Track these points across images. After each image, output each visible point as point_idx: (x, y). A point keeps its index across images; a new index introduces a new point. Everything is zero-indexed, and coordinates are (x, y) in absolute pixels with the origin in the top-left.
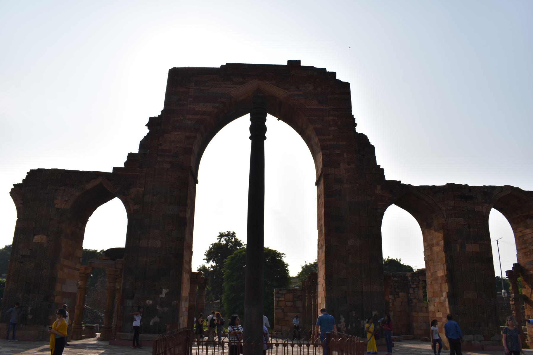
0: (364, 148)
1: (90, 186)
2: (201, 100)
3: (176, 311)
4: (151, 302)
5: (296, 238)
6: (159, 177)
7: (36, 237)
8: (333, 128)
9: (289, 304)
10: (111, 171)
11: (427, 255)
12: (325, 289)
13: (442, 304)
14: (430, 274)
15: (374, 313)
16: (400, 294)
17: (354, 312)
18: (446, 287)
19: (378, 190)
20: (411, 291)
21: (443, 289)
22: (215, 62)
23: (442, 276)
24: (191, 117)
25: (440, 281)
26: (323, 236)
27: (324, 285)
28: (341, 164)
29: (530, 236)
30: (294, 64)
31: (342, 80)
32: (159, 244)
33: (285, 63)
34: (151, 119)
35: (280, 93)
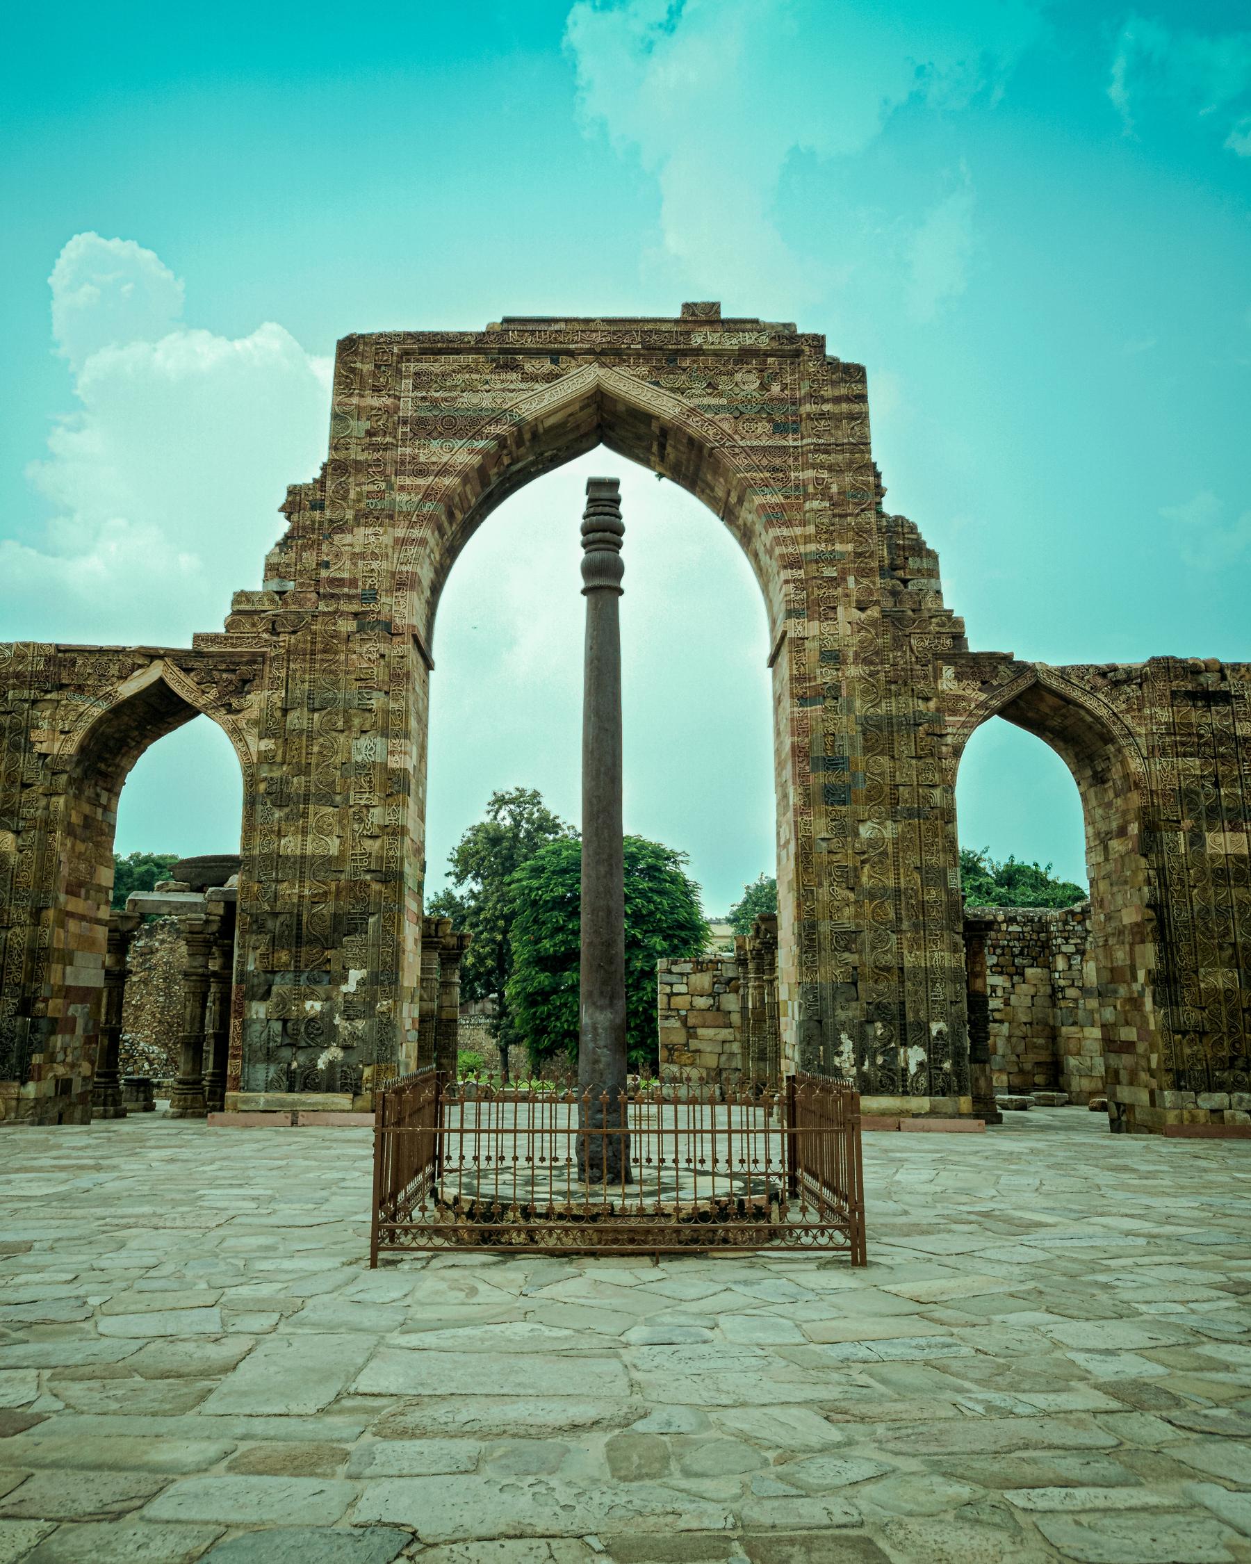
1: (127, 689)
3: (387, 1029)
4: (318, 1006)
5: (720, 816)
14: (1102, 917)
15: (935, 1027)
17: (879, 1025)
19: (948, 680)
23: (1137, 924)
25: (1128, 938)
26: (790, 814)
27: (795, 949)
28: (840, 609)
30: (704, 315)
31: (845, 359)
32: (334, 846)
33: (677, 314)
34: (293, 491)
35: (662, 403)
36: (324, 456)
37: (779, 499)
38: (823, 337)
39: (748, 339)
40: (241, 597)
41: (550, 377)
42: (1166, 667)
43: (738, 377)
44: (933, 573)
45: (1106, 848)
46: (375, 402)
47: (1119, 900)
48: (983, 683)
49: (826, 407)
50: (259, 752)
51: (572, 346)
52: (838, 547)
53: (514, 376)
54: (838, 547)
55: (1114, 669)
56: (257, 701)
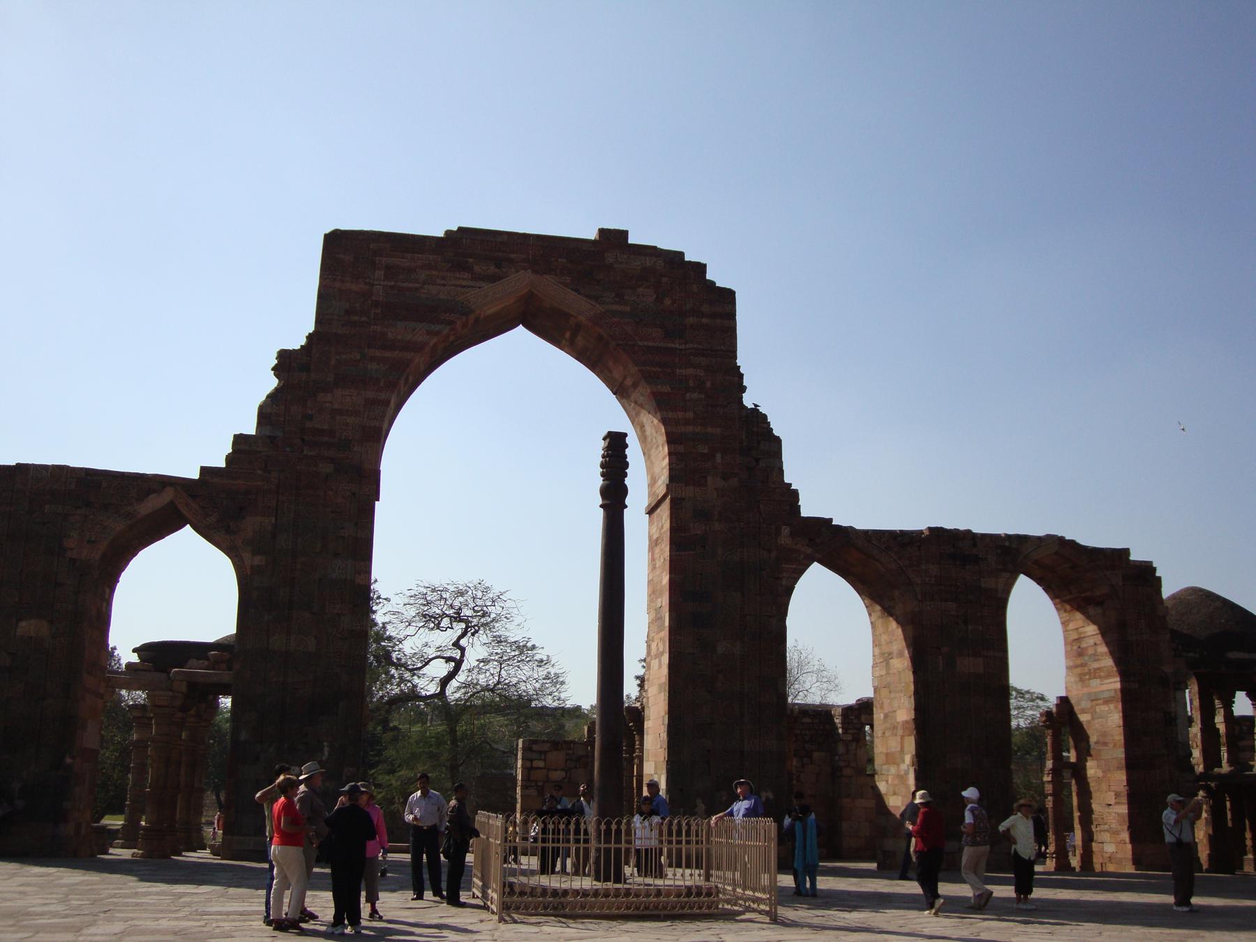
0: (757, 442)
2: (392, 308)
6: (299, 487)
7: (23, 624)
8: (695, 396)
9: (557, 775)
10: (196, 476)
11: (877, 674)
12: (665, 746)
13: (902, 778)
14: (882, 716)
16: (816, 755)
18: (910, 744)
20: (841, 749)
21: (906, 749)
22: (432, 223)
23: (907, 722)
24: (378, 354)
25: (900, 732)
27: (664, 736)
28: (709, 479)
29: (1091, 641)
30: (613, 239)
34: (284, 355)
36: (311, 329)
37: (666, 389)
38: (705, 266)
39: (648, 262)
40: (239, 440)
41: (494, 279)
42: (937, 534)
43: (640, 290)
44: (778, 454)
45: (888, 664)
46: (354, 287)
47: (896, 704)
48: (810, 540)
49: (705, 320)
50: (252, 567)
51: (513, 256)
52: (709, 430)
53: (466, 275)
54: (709, 430)
55: (903, 533)
56: (252, 524)
